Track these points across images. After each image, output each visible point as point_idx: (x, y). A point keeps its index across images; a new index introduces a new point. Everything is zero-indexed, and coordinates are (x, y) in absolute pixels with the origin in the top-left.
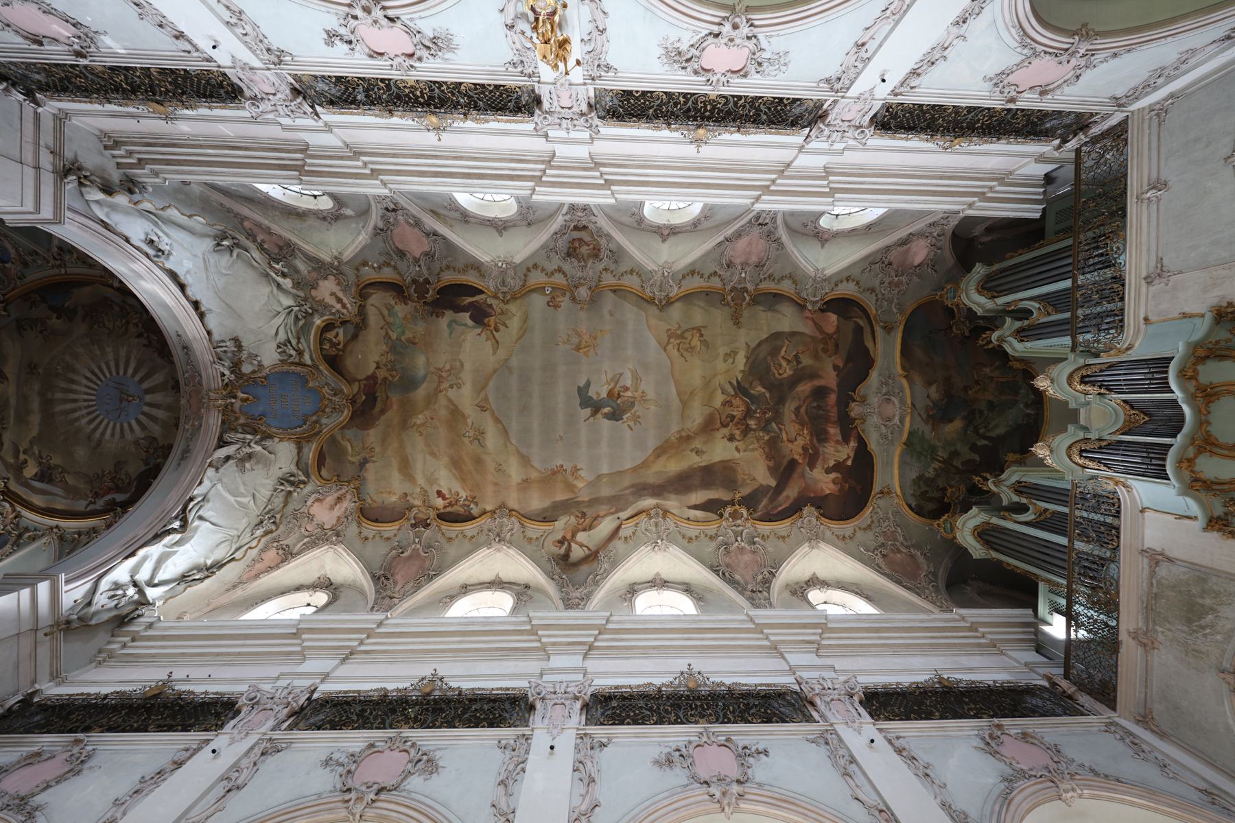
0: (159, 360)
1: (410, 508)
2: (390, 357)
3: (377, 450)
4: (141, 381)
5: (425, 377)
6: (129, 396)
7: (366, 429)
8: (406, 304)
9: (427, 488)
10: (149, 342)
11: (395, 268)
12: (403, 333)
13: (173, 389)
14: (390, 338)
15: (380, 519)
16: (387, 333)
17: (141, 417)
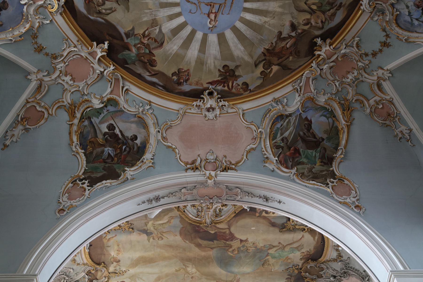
0: (260, 50)
1: (106, 267)
2: (251, 250)
3: (161, 242)
4: (235, 30)
5: (232, 273)
6: (216, 14)
7: (181, 234)
8: (301, 259)
9: (126, 275)
10: (284, 39)
11: (335, 260)
12: (274, 257)
13: (225, 66)
14: (270, 249)
15: (92, 247)
16: (274, 247)
17: (188, 30)
